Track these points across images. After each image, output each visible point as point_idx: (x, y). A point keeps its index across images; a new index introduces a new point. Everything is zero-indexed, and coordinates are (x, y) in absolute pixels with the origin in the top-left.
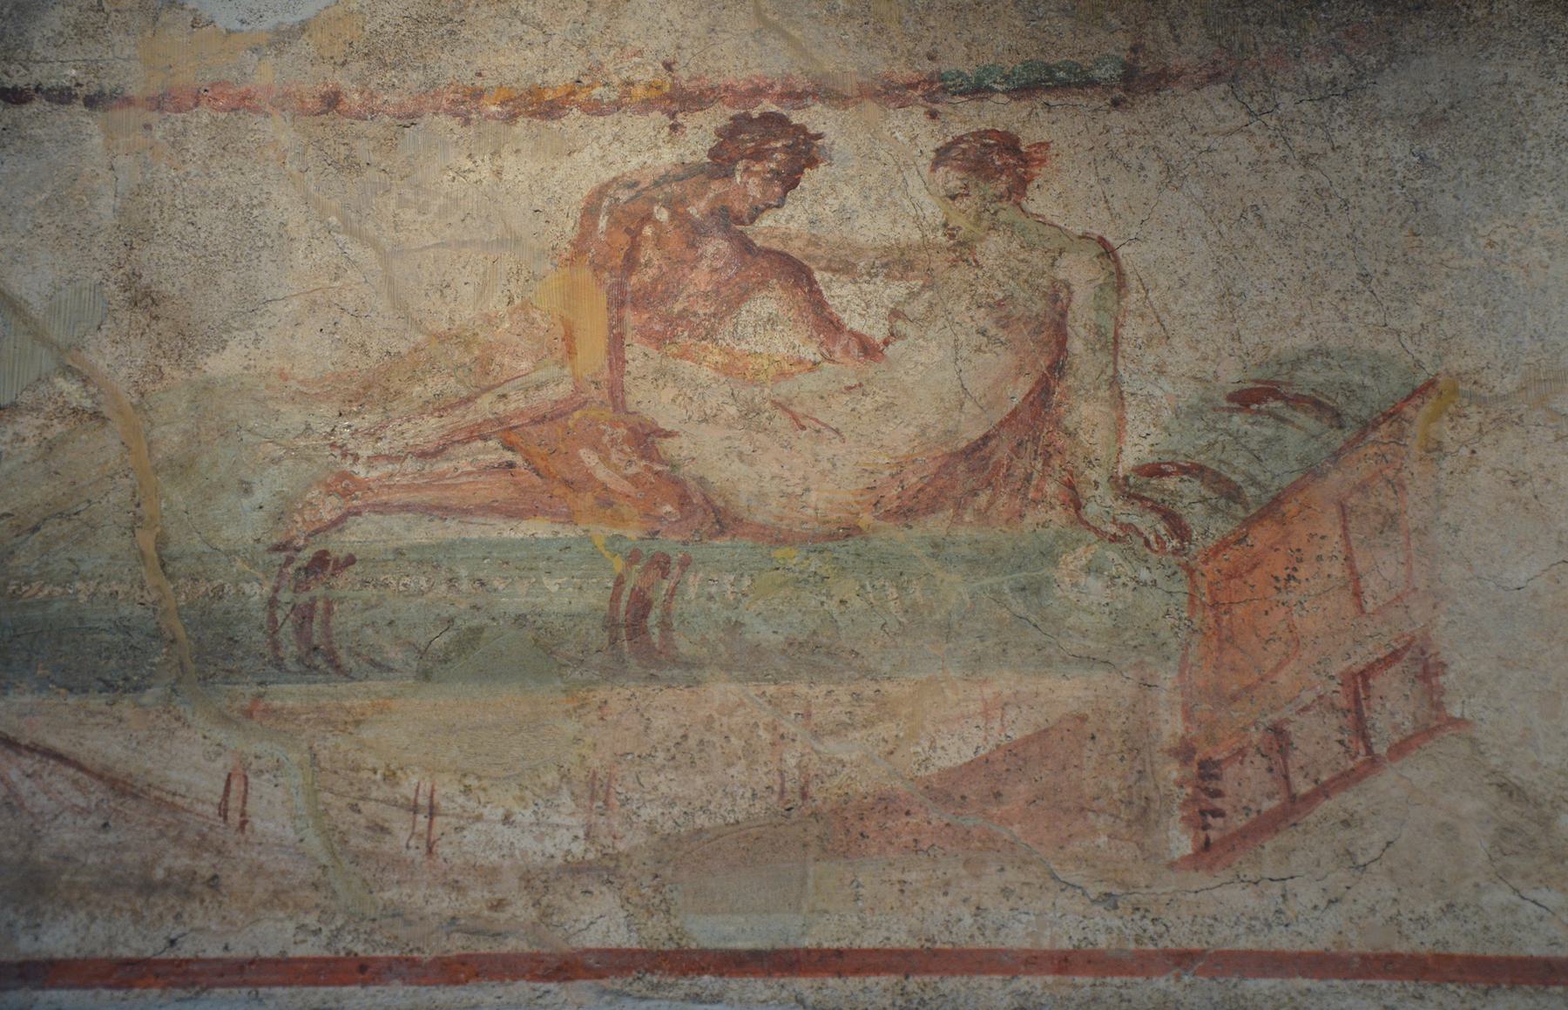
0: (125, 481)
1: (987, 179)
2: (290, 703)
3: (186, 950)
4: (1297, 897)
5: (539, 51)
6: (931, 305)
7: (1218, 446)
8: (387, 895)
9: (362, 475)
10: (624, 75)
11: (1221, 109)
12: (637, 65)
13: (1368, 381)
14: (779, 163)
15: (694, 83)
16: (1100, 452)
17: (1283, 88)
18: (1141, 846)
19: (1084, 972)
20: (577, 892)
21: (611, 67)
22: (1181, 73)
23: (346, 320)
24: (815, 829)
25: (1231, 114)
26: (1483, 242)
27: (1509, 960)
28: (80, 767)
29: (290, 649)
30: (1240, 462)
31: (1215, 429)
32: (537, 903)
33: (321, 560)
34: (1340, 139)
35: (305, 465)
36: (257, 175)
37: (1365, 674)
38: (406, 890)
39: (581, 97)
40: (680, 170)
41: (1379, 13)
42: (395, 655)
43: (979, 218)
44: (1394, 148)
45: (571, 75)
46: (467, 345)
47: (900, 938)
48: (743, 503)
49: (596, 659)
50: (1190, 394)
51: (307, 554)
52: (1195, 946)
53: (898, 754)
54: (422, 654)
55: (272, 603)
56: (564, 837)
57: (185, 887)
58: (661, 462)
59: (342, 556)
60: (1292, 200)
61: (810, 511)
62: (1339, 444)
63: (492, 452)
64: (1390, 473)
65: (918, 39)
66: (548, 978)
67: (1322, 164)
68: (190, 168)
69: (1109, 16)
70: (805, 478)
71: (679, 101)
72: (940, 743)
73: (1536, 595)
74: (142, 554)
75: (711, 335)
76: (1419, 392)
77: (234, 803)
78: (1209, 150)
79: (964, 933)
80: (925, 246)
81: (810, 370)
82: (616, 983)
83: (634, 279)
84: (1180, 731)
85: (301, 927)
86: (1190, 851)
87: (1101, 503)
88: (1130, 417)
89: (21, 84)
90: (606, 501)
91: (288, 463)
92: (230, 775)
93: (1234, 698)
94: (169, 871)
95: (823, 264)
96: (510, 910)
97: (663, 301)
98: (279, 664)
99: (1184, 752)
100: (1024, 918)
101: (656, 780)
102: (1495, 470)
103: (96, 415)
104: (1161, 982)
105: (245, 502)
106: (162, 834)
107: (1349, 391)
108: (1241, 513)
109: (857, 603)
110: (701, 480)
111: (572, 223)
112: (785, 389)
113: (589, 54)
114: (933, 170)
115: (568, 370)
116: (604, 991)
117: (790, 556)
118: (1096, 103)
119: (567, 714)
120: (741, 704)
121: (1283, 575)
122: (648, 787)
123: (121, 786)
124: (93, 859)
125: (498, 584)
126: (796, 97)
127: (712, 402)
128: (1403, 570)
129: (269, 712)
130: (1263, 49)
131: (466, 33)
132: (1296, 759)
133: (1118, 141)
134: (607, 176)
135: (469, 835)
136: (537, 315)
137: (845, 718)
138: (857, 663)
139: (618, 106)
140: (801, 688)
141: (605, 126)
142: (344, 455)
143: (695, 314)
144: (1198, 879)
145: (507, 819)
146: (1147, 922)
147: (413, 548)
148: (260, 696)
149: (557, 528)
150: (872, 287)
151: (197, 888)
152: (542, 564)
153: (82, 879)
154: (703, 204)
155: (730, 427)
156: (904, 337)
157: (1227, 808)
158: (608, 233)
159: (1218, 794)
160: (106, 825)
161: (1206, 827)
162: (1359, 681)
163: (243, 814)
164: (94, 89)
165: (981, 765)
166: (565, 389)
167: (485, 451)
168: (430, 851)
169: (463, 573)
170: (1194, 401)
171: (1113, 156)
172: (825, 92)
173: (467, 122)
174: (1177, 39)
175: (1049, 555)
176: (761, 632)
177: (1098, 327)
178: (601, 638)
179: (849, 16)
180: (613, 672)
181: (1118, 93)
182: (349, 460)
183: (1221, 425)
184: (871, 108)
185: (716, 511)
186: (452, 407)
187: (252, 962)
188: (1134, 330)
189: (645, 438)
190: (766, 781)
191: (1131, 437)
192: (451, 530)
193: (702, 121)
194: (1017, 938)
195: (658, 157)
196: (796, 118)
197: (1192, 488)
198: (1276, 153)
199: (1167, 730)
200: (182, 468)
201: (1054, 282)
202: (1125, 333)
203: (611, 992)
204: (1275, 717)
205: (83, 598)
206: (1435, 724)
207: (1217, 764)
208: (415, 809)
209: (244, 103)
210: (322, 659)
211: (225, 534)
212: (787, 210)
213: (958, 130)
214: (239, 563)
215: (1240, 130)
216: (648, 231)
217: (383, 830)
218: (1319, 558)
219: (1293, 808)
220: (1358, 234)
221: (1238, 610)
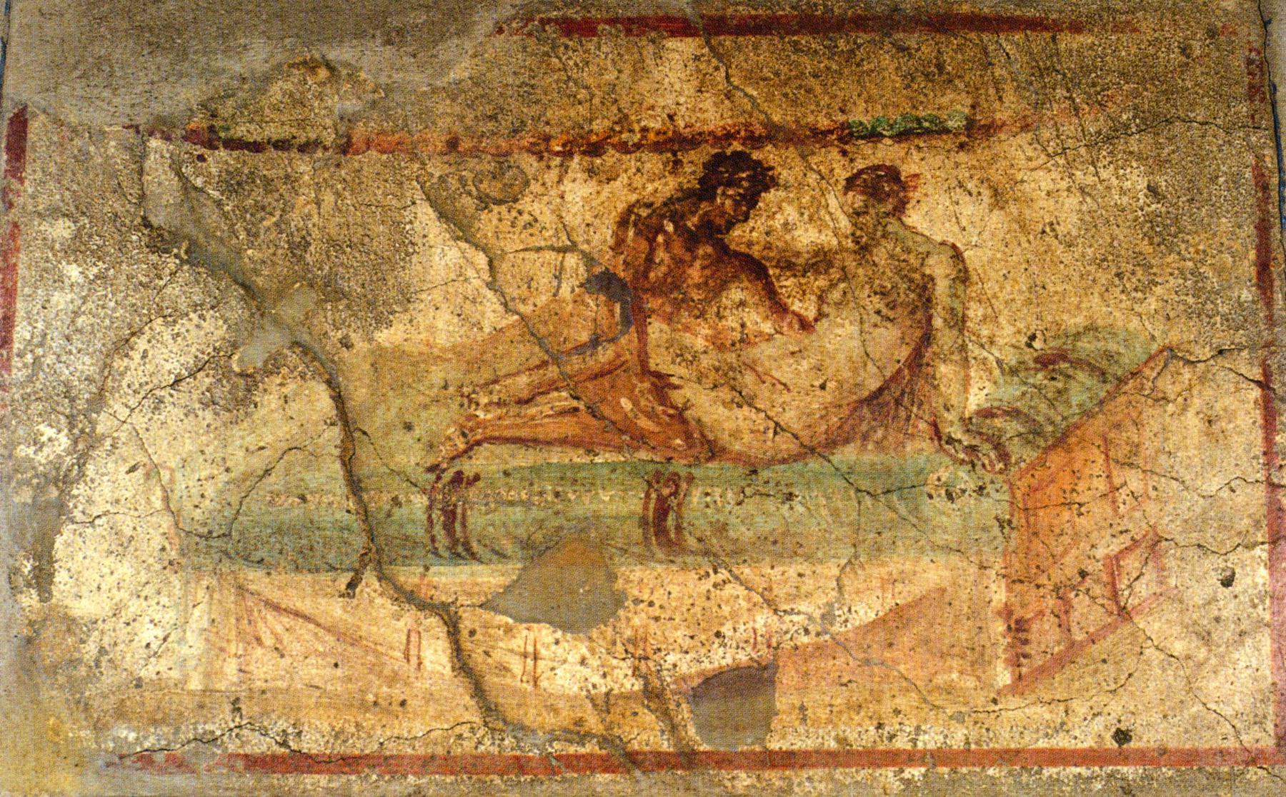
1: (881, 201)
7: (1028, 396)
10: (643, 124)
13: (1122, 350)
14: (745, 189)
15: (688, 130)
16: (954, 401)
18: (979, 678)
22: (1004, 124)
26: (1192, 250)
31: (1025, 383)
33: (458, 478)
34: (1104, 174)
37: (1117, 558)
39: (615, 140)
40: (679, 194)
42: (509, 547)
45: (607, 123)
48: (725, 439)
49: (636, 550)
59: (471, 475)
62: (1103, 394)
64: (1134, 415)
72: (853, 609)
75: (702, 315)
77: (413, 651)
78: (1022, 181)
80: (842, 249)
81: (768, 340)
86: (1009, 682)
88: (973, 374)
92: (409, 631)
94: (376, 695)
98: (436, 552)
107: (1109, 356)
111: (610, 232)
114: (845, 194)
122: (671, 640)
126: (755, 141)
134: (633, 198)
137: (794, 591)
139: (638, 146)
141: (630, 161)
144: (1014, 702)
156: (827, 316)
157: (1033, 652)
158: (633, 240)
159: (1026, 642)
163: (419, 658)
164: (303, 140)
168: (535, 684)
170: (1013, 363)
171: (961, 185)
177: (952, 309)
178: (637, 533)
181: (963, 139)
182: (473, 406)
183: (1031, 381)
185: (709, 441)
186: (538, 367)
188: (975, 312)
191: (973, 390)
193: (694, 158)
197: (1012, 427)
198: (1064, 185)
199: (996, 598)
201: (923, 275)
202: (971, 313)
207: (1027, 621)
208: (525, 656)
212: (751, 223)
213: (860, 164)
215: (1040, 168)
216: (660, 239)
217: (506, 669)
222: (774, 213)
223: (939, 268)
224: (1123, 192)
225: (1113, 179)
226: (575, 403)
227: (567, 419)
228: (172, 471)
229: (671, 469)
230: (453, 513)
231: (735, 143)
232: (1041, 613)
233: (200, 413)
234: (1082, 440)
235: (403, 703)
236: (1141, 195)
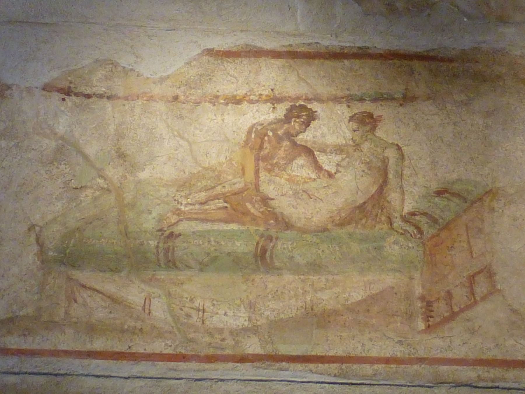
0: (116, 209)
2: (163, 277)
4: (453, 342)
6: (348, 162)
9: (183, 209)
10: (259, 92)
12: (263, 90)
16: (398, 208)
21: (256, 90)
33: (172, 234)
35: (166, 206)
37: (473, 276)
40: (276, 121)
42: (192, 263)
45: (244, 92)
46: (213, 171)
51: (167, 233)
54: (200, 263)
55: (157, 247)
58: (270, 208)
59: (177, 233)
61: (313, 223)
63: (220, 203)
70: (312, 214)
71: (275, 100)
74: (121, 231)
75: (284, 170)
80: (346, 145)
83: (262, 153)
87: (398, 223)
91: (162, 205)
93: (436, 283)
95: (317, 149)
98: (160, 266)
101: (269, 303)
102: (509, 216)
105: (150, 216)
108: (438, 227)
109: (327, 251)
112: (306, 186)
113: (249, 86)
115: (243, 179)
117: (308, 237)
119: (243, 283)
120: (294, 281)
121: (450, 246)
125: (223, 243)
134: (255, 122)
136: (234, 163)
139: (257, 101)
140: (311, 277)
141: (254, 107)
142: (178, 203)
143: (280, 163)
148: (154, 275)
149: (240, 226)
150: (331, 157)
152: (235, 237)
154: (282, 131)
155: (290, 197)
158: (255, 139)
160: (111, 312)
162: (472, 279)
167: (219, 203)
169: (212, 239)
175: (383, 238)
176: (299, 259)
178: (253, 260)
182: (180, 205)
185: (286, 223)
186: (209, 189)
189: (265, 200)
191: (406, 204)
192: (208, 226)
195: (269, 117)
196: (309, 106)
199: (417, 292)
200: (132, 206)
203: (256, 367)
204: (448, 288)
205: (104, 244)
206: (493, 291)
210: (171, 264)
212: (306, 133)
214: (148, 234)
216: (266, 138)
221: (437, 256)
222: (317, 130)
226: (226, 205)
228: (41, 227)
230: (168, 248)
231: (300, 101)
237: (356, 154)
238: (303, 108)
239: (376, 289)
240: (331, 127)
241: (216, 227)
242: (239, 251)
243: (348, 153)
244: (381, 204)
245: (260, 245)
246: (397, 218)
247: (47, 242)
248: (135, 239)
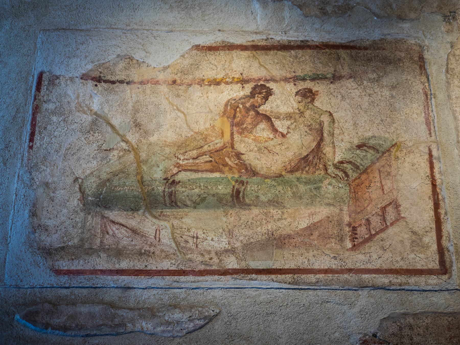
1: (306, 98)
2: (168, 213)
3: (149, 268)
5: (215, 71)
8: (188, 256)
10: (233, 76)
11: (352, 84)
13: (383, 143)
17: (364, 80)
18: (341, 246)
19: (330, 274)
20: (227, 256)
23: (178, 129)
24: (275, 242)
25: (354, 85)
26: (405, 113)
27: (414, 269)
28: (127, 227)
29: (168, 201)
30: (359, 161)
31: (353, 153)
32: (219, 258)
33: (174, 182)
34: (376, 91)
36: (160, 98)
37: (385, 207)
38: (192, 255)
39: (224, 81)
40: (244, 97)
41: (382, 64)
42: (189, 203)
43: (305, 107)
44: (386, 93)
45: (222, 76)
47: (293, 266)
48: (258, 169)
49: (229, 204)
50: (348, 146)
51: (171, 180)
52: (353, 268)
53: (291, 225)
54: (194, 203)
55: (164, 191)
56: (224, 243)
57: (147, 254)
58: (242, 160)
60: (367, 104)
61: (272, 171)
62: (378, 157)
64: (388, 163)
65: (291, 68)
66: (221, 275)
67: (373, 96)
68: (146, 97)
69: (329, 64)
71: (243, 82)
72: (300, 223)
73: (417, 190)
75: (251, 132)
76: (393, 146)
77: (157, 236)
79: (306, 265)
80: (294, 113)
82: (235, 276)
84: (348, 220)
85: (171, 263)
87: (331, 170)
88: (336, 151)
89: (114, 80)
90: (231, 169)
91: (166, 161)
93: (359, 213)
94: (145, 250)
96: (213, 260)
97: (241, 125)
98: (166, 205)
99: (349, 225)
100: (318, 262)
103: (129, 151)
104: (346, 276)
105: (158, 169)
106: (143, 243)
107: (380, 145)
108: (359, 172)
109: (282, 192)
110: (250, 164)
112: (267, 144)
115: (222, 140)
116: (233, 278)
118: (327, 82)
121: (368, 186)
122: (241, 233)
123: (134, 231)
124: (130, 248)
126: (267, 81)
127: (252, 147)
128: (392, 184)
129: (164, 215)
130: (360, 71)
131: (201, 67)
132: (372, 226)
133: (332, 91)
134: (230, 98)
135: (205, 243)
137: (280, 217)
138: (282, 205)
139: (231, 83)
141: (229, 87)
144: (353, 253)
145: (212, 240)
146: (343, 262)
147: (192, 179)
148: (162, 212)
149: (221, 175)
151: (151, 254)
153: (128, 252)
156: (290, 133)
157: (358, 237)
158: (230, 110)
159: (356, 234)
161: (354, 241)
162: (384, 209)
164: (128, 80)
165: (308, 228)
166: (222, 144)
168: (197, 247)
169: (202, 185)
170: (349, 147)
171: (331, 94)
172: (273, 80)
173: (201, 86)
174: (343, 69)
175: (321, 181)
178: (231, 199)
179: (277, 63)
180: (233, 206)
181: (332, 80)
182: (179, 160)
183: (355, 152)
184: (282, 83)
185: (253, 171)
186: (199, 148)
187: (162, 270)
188: (337, 132)
189: (238, 155)
190: (265, 232)
191: (337, 155)
192: (199, 175)
194: (316, 266)
195: (240, 93)
196: (267, 85)
198: (364, 94)
199: (346, 220)
200: (146, 162)
201: (320, 121)
202: (335, 132)
204: (367, 217)
205: (127, 190)
206: (399, 218)
207: (356, 227)
208: (194, 237)
209: (157, 83)
211: (154, 176)
216: (238, 110)
217: (188, 242)
218: (375, 182)
219: (371, 237)
220: (380, 111)
221: (359, 193)
223: (325, 119)
224: (382, 96)
225: (379, 93)
226: (211, 159)
227: (208, 164)
229: (241, 179)
232: (360, 225)
233: (92, 161)
234: (372, 170)
235: (153, 253)
236: (388, 97)
237: (302, 119)
238: (263, 86)
239: (316, 219)
240: (284, 100)
241: (205, 175)
242: (221, 193)
243: (295, 119)
244: (319, 156)
245: (235, 189)
246: (330, 165)
247: (87, 190)
248: (148, 186)
